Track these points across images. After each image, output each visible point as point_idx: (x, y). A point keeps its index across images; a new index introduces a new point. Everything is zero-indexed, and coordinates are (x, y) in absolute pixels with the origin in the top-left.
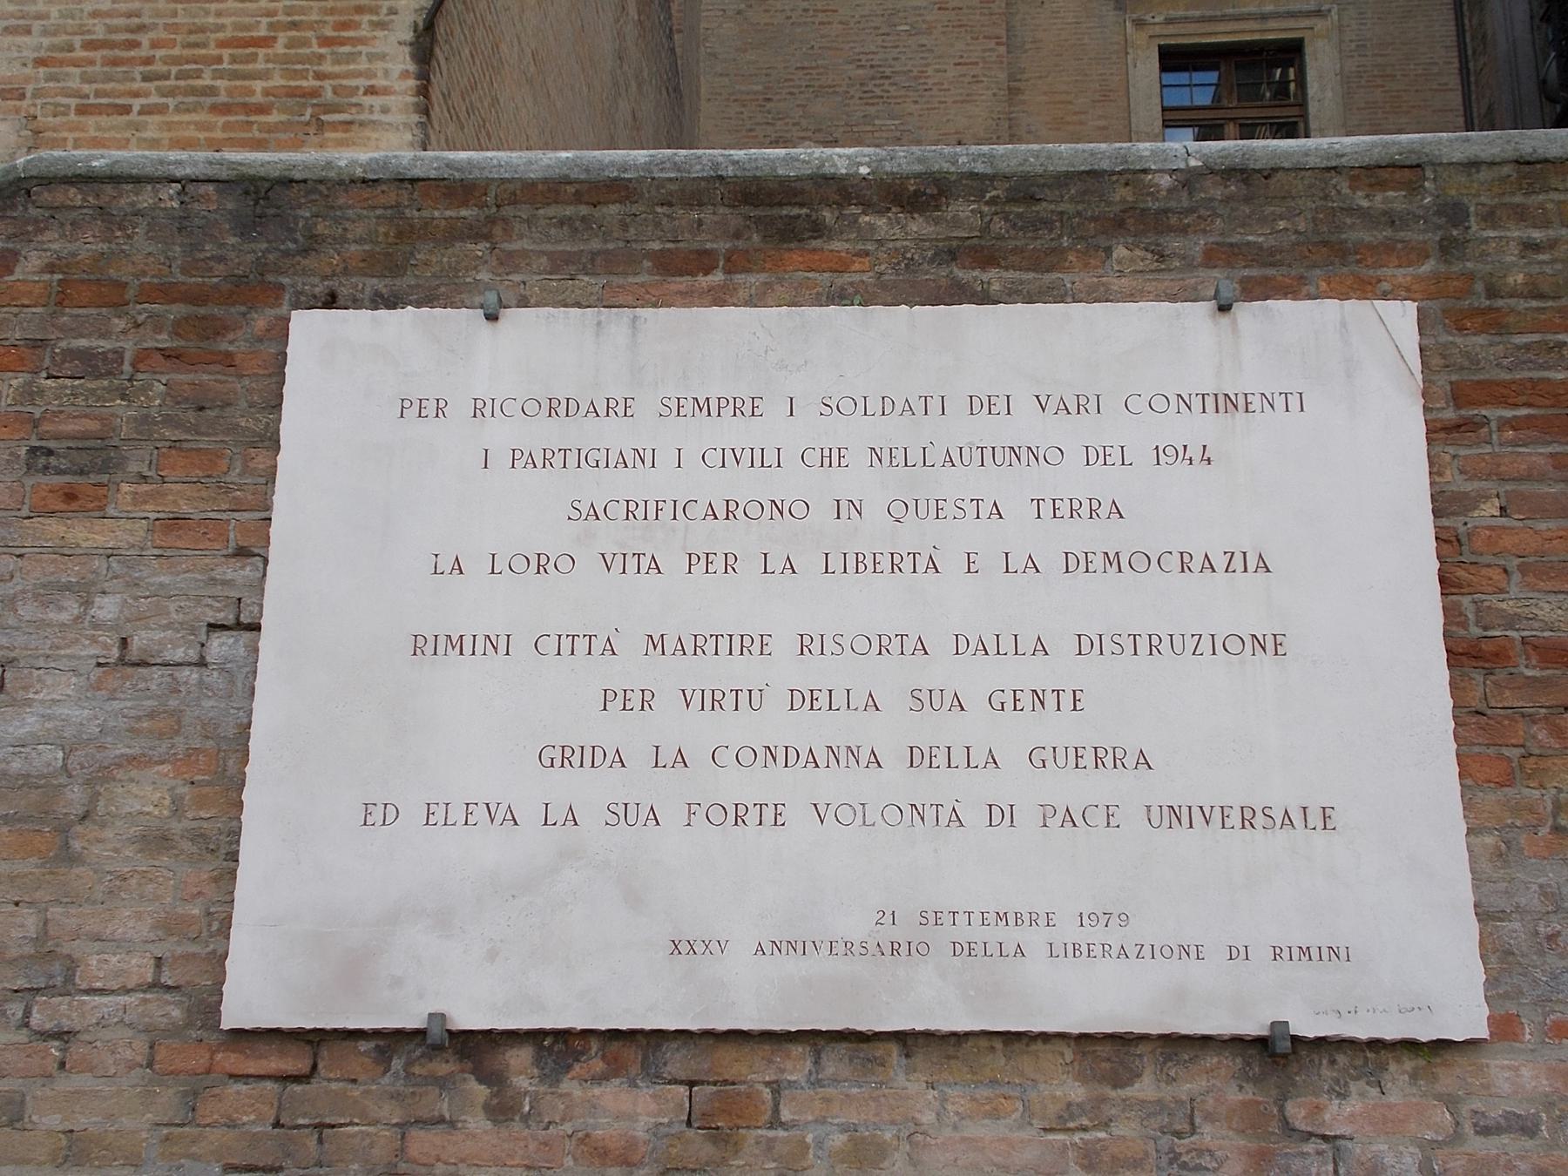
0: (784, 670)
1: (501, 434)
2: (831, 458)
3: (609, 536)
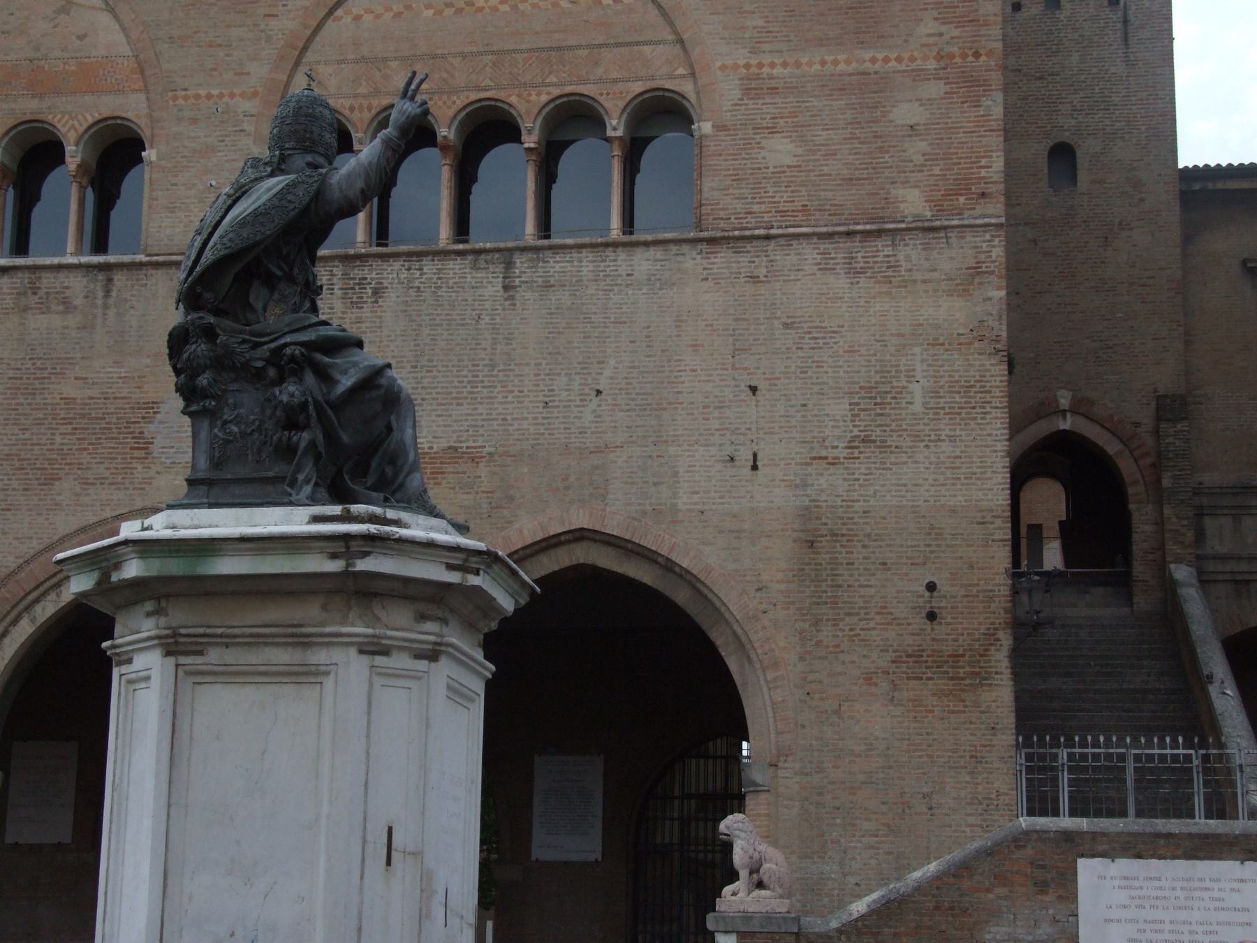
0: (1167, 927)
1: (1116, 883)
2: (1174, 889)
3: (1137, 902)
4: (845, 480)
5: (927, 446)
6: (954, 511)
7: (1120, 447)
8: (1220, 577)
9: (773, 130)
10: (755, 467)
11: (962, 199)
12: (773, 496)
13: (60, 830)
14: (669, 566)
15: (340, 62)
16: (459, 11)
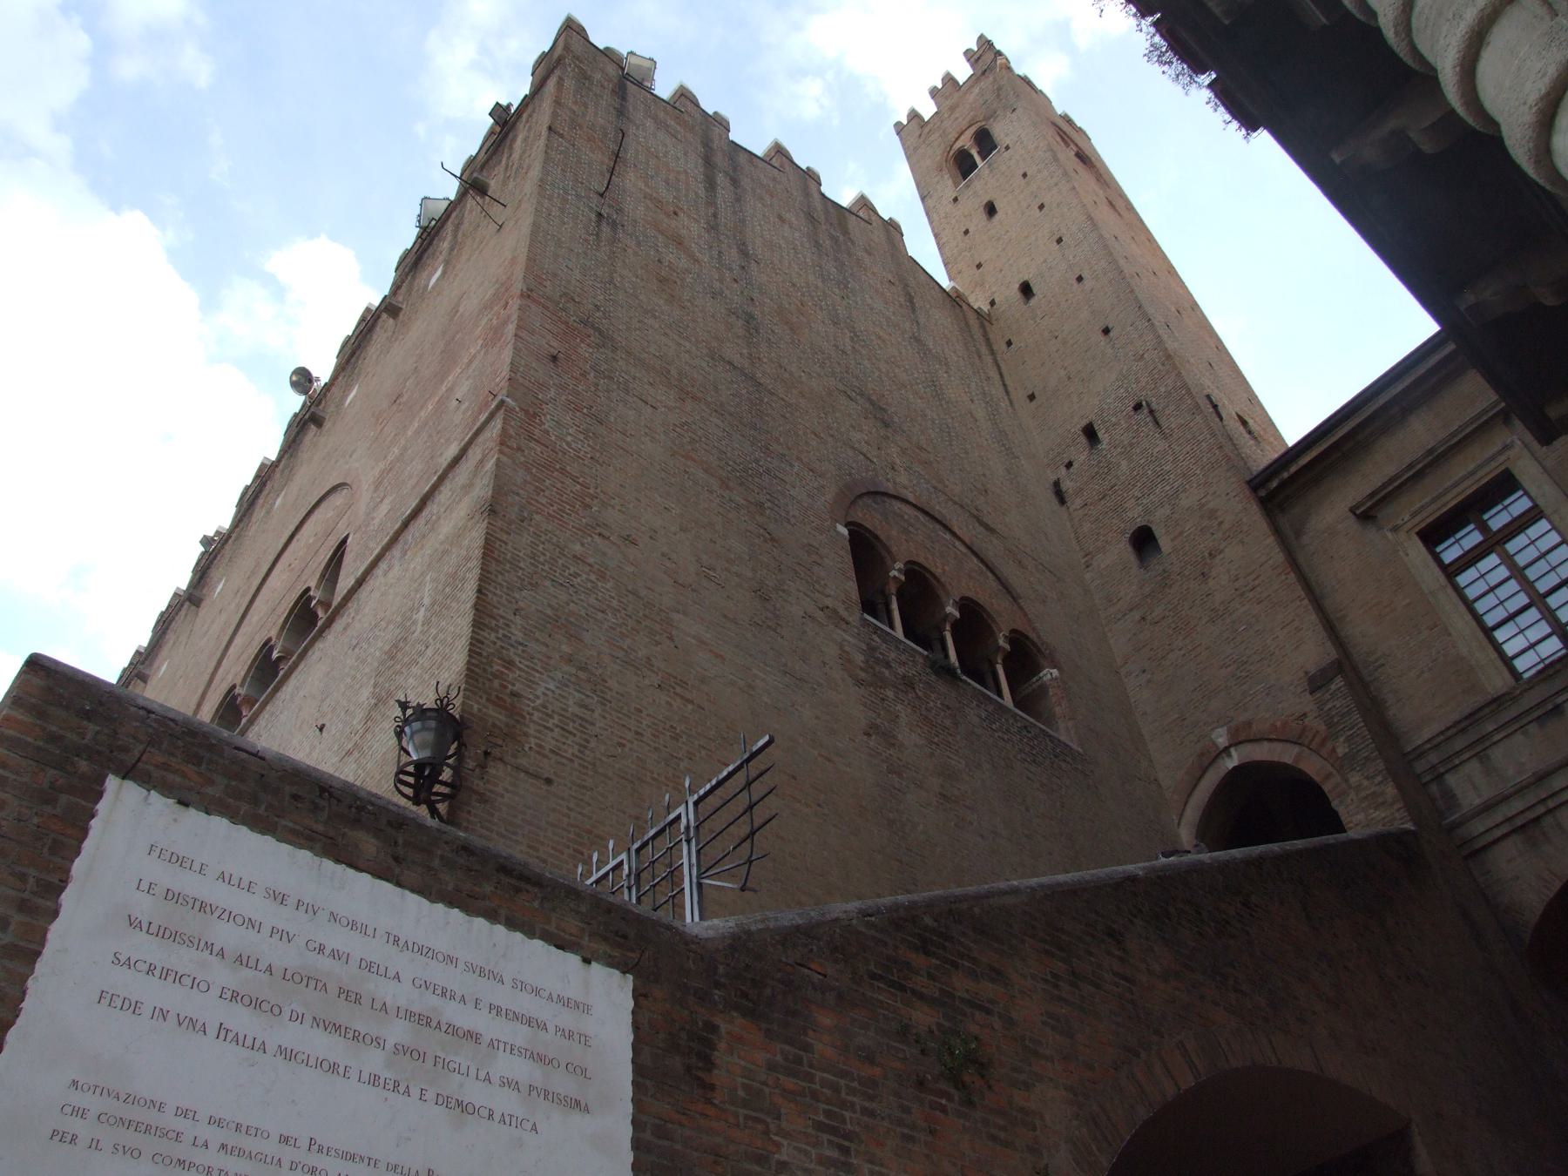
7: (1296, 749)
8: (1498, 833)
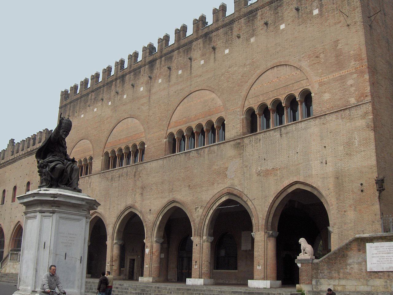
0: (385, 258)
1: (374, 248)
3: (379, 252)
4: (343, 163)
5: (359, 153)
6: (365, 167)
9: (325, 92)
10: (326, 164)
11: (362, 98)
12: (330, 169)
13: (249, 248)
14: (312, 187)
15: (252, 98)
16: (270, 83)
